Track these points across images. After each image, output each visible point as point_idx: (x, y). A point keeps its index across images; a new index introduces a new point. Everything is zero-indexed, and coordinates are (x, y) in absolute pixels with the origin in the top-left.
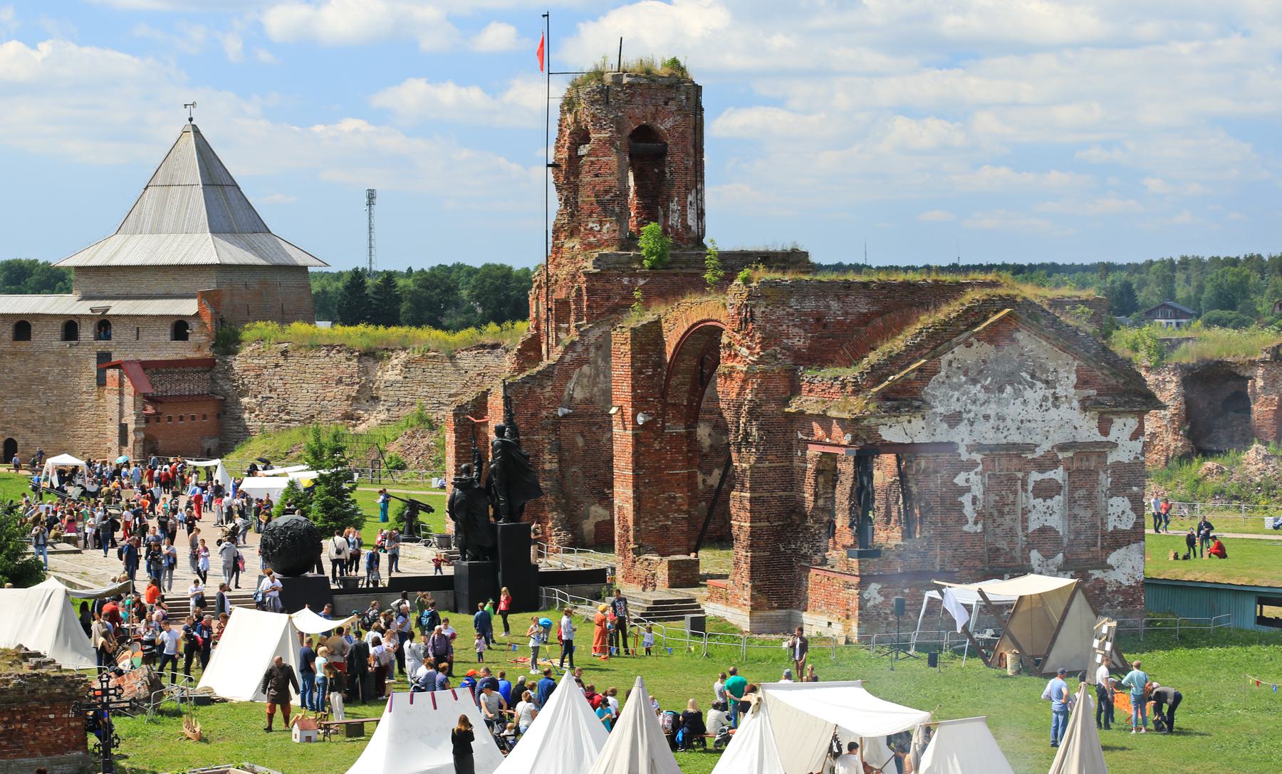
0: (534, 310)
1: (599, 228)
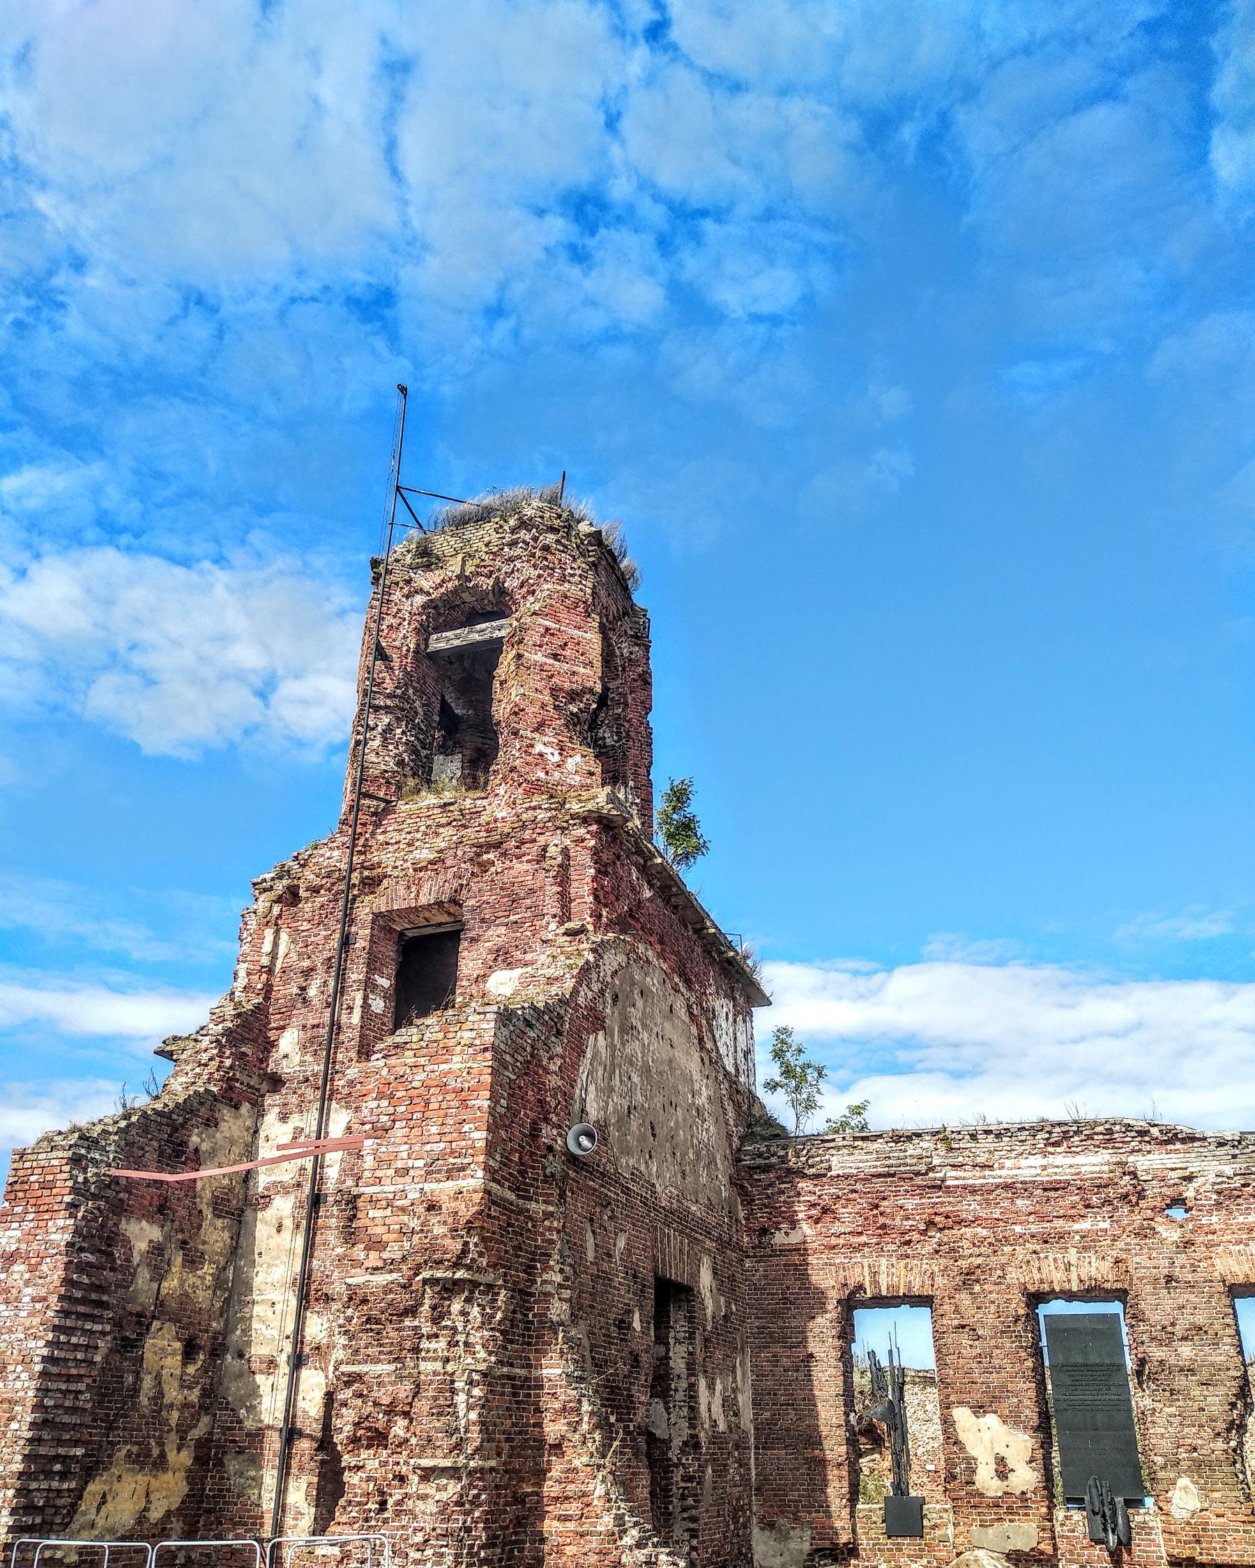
0: (267, 947)
1: (557, 758)
